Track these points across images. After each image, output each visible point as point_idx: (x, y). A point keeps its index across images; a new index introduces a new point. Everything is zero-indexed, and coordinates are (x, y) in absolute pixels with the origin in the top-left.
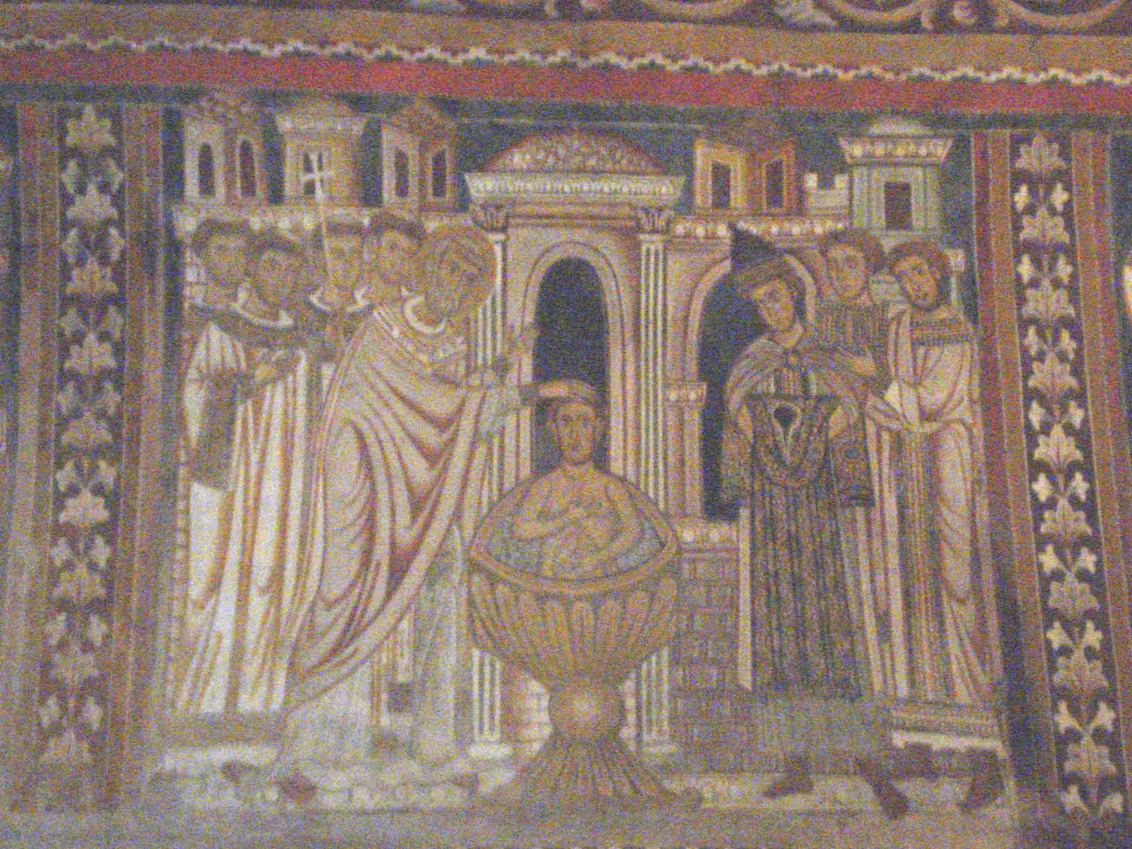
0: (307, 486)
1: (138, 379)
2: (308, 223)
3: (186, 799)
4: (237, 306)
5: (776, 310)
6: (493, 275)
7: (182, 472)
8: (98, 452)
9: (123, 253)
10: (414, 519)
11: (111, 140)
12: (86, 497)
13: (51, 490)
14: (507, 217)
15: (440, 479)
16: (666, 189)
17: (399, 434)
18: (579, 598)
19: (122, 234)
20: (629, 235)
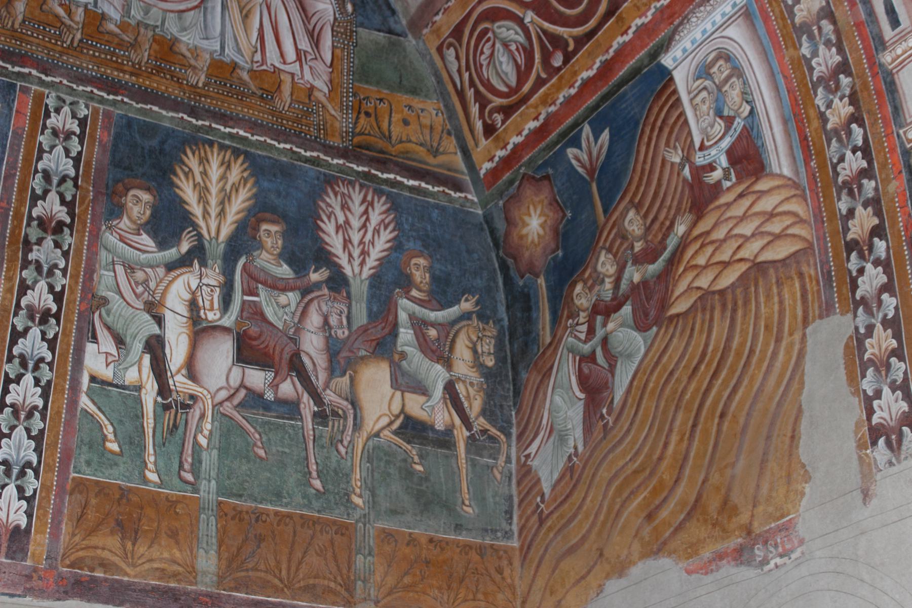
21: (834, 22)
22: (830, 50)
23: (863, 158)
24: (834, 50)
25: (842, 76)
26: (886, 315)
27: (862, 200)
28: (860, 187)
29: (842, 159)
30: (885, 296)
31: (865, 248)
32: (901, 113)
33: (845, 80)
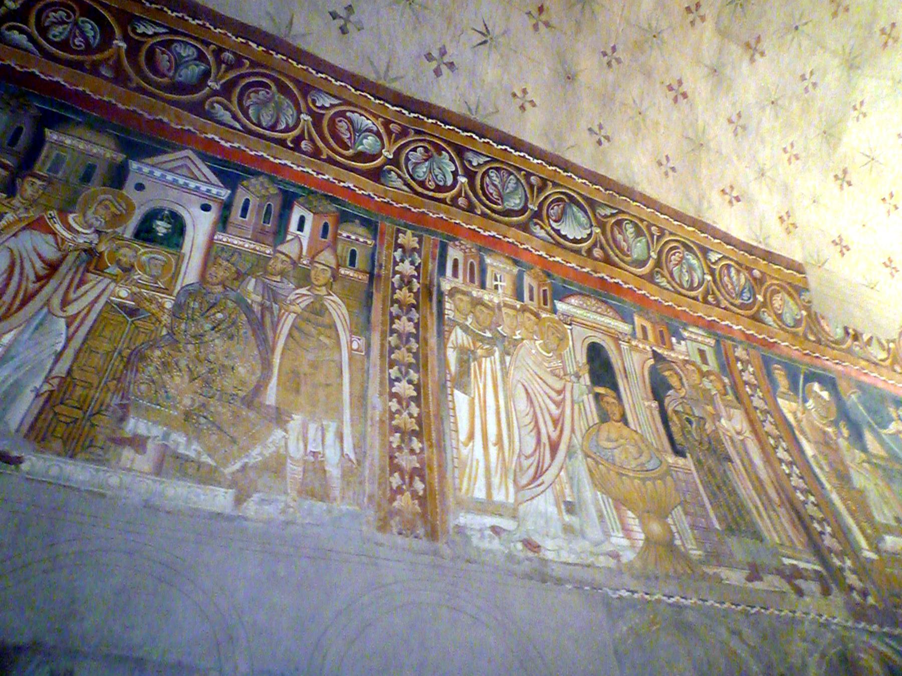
0: (506, 404)
1: (426, 340)
2: (496, 300)
3: (475, 541)
4: (468, 323)
5: (674, 381)
6: (568, 339)
7: (449, 384)
8: (410, 365)
9: (419, 289)
10: (555, 427)
11: (417, 246)
12: (404, 383)
13: (387, 377)
14: (571, 320)
15: (563, 412)
16: (625, 328)
17: (542, 392)
18: (635, 478)
20: (616, 340)
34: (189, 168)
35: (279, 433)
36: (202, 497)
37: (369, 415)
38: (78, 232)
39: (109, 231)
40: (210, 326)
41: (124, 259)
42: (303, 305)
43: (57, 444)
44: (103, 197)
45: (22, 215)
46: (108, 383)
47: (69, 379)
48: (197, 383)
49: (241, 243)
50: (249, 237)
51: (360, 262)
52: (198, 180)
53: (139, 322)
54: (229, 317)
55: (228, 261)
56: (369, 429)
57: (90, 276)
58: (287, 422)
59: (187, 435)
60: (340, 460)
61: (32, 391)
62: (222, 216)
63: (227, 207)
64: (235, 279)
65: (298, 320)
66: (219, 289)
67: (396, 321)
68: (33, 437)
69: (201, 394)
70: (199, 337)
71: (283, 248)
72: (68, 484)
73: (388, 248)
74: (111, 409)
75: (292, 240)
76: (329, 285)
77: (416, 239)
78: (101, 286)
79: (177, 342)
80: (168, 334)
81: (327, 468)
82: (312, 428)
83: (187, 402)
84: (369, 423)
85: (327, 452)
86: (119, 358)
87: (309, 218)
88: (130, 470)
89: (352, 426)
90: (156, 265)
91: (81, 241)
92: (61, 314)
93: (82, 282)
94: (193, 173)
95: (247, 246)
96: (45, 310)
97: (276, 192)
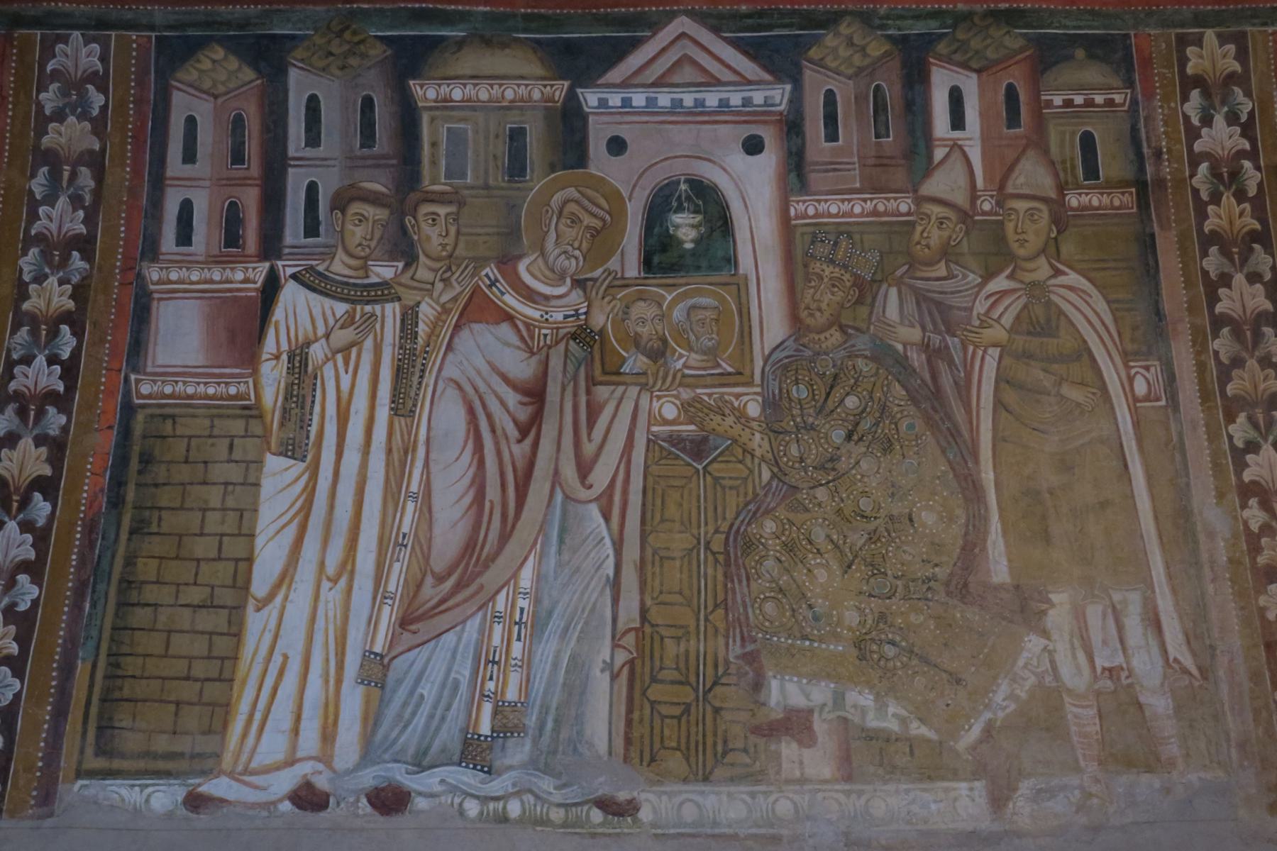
9: (1260, 185)
11: (1237, 67)
13: (1227, 447)
19: (1258, 168)
21: (99, 177)
22: (75, 210)
23: (60, 378)
24: (81, 213)
25: (75, 254)
26: (15, 604)
27: (35, 432)
28: (41, 413)
29: (27, 360)
30: (23, 578)
31: (15, 498)
32: (142, 353)
33: (77, 261)
34: (694, 63)
35: (1034, 643)
36: (933, 807)
37: (1205, 556)
38: (547, 298)
39: (597, 273)
40: (842, 433)
41: (645, 331)
42: (1008, 320)
43: (675, 762)
44: (558, 198)
45: (445, 298)
46: (711, 618)
47: (648, 629)
48: (859, 571)
49: (845, 207)
50: (858, 185)
51: (1111, 163)
52: (718, 82)
53: (715, 465)
54: (871, 397)
55: (832, 262)
56: (1210, 589)
57: (602, 392)
58: (1044, 613)
59: (871, 688)
60: (1165, 676)
61: (602, 671)
62: (790, 153)
63: (792, 126)
64: (859, 301)
65: (1007, 361)
66: (835, 337)
67: (1222, 291)
68: (634, 754)
69: (871, 595)
70: (829, 463)
71: (933, 186)
72: (717, 831)
73: (1166, 98)
74: (733, 670)
75: (947, 156)
76: (1051, 249)
77: (1231, 48)
78: (627, 408)
79: (795, 488)
80: (774, 475)
81: (1142, 699)
82: (1094, 613)
83: (852, 618)
84: (1207, 570)
85: (1135, 663)
86: (710, 558)
87: (970, 85)
88: (803, 781)
89: (1174, 591)
90: (702, 322)
91: (560, 317)
92: (583, 494)
93: (593, 413)
94: (704, 70)
95: (857, 210)
96: (559, 497)
97: (886, 47)
